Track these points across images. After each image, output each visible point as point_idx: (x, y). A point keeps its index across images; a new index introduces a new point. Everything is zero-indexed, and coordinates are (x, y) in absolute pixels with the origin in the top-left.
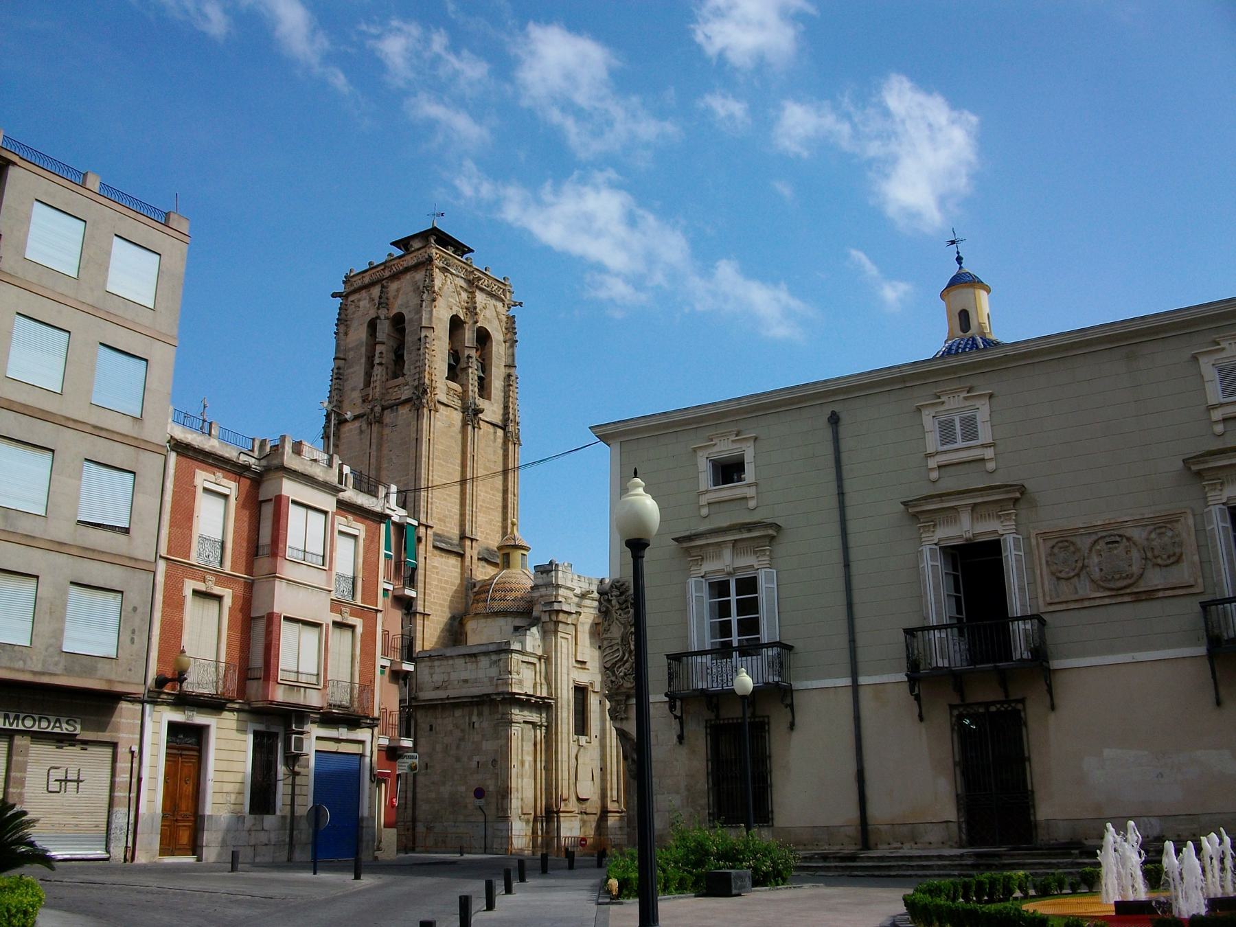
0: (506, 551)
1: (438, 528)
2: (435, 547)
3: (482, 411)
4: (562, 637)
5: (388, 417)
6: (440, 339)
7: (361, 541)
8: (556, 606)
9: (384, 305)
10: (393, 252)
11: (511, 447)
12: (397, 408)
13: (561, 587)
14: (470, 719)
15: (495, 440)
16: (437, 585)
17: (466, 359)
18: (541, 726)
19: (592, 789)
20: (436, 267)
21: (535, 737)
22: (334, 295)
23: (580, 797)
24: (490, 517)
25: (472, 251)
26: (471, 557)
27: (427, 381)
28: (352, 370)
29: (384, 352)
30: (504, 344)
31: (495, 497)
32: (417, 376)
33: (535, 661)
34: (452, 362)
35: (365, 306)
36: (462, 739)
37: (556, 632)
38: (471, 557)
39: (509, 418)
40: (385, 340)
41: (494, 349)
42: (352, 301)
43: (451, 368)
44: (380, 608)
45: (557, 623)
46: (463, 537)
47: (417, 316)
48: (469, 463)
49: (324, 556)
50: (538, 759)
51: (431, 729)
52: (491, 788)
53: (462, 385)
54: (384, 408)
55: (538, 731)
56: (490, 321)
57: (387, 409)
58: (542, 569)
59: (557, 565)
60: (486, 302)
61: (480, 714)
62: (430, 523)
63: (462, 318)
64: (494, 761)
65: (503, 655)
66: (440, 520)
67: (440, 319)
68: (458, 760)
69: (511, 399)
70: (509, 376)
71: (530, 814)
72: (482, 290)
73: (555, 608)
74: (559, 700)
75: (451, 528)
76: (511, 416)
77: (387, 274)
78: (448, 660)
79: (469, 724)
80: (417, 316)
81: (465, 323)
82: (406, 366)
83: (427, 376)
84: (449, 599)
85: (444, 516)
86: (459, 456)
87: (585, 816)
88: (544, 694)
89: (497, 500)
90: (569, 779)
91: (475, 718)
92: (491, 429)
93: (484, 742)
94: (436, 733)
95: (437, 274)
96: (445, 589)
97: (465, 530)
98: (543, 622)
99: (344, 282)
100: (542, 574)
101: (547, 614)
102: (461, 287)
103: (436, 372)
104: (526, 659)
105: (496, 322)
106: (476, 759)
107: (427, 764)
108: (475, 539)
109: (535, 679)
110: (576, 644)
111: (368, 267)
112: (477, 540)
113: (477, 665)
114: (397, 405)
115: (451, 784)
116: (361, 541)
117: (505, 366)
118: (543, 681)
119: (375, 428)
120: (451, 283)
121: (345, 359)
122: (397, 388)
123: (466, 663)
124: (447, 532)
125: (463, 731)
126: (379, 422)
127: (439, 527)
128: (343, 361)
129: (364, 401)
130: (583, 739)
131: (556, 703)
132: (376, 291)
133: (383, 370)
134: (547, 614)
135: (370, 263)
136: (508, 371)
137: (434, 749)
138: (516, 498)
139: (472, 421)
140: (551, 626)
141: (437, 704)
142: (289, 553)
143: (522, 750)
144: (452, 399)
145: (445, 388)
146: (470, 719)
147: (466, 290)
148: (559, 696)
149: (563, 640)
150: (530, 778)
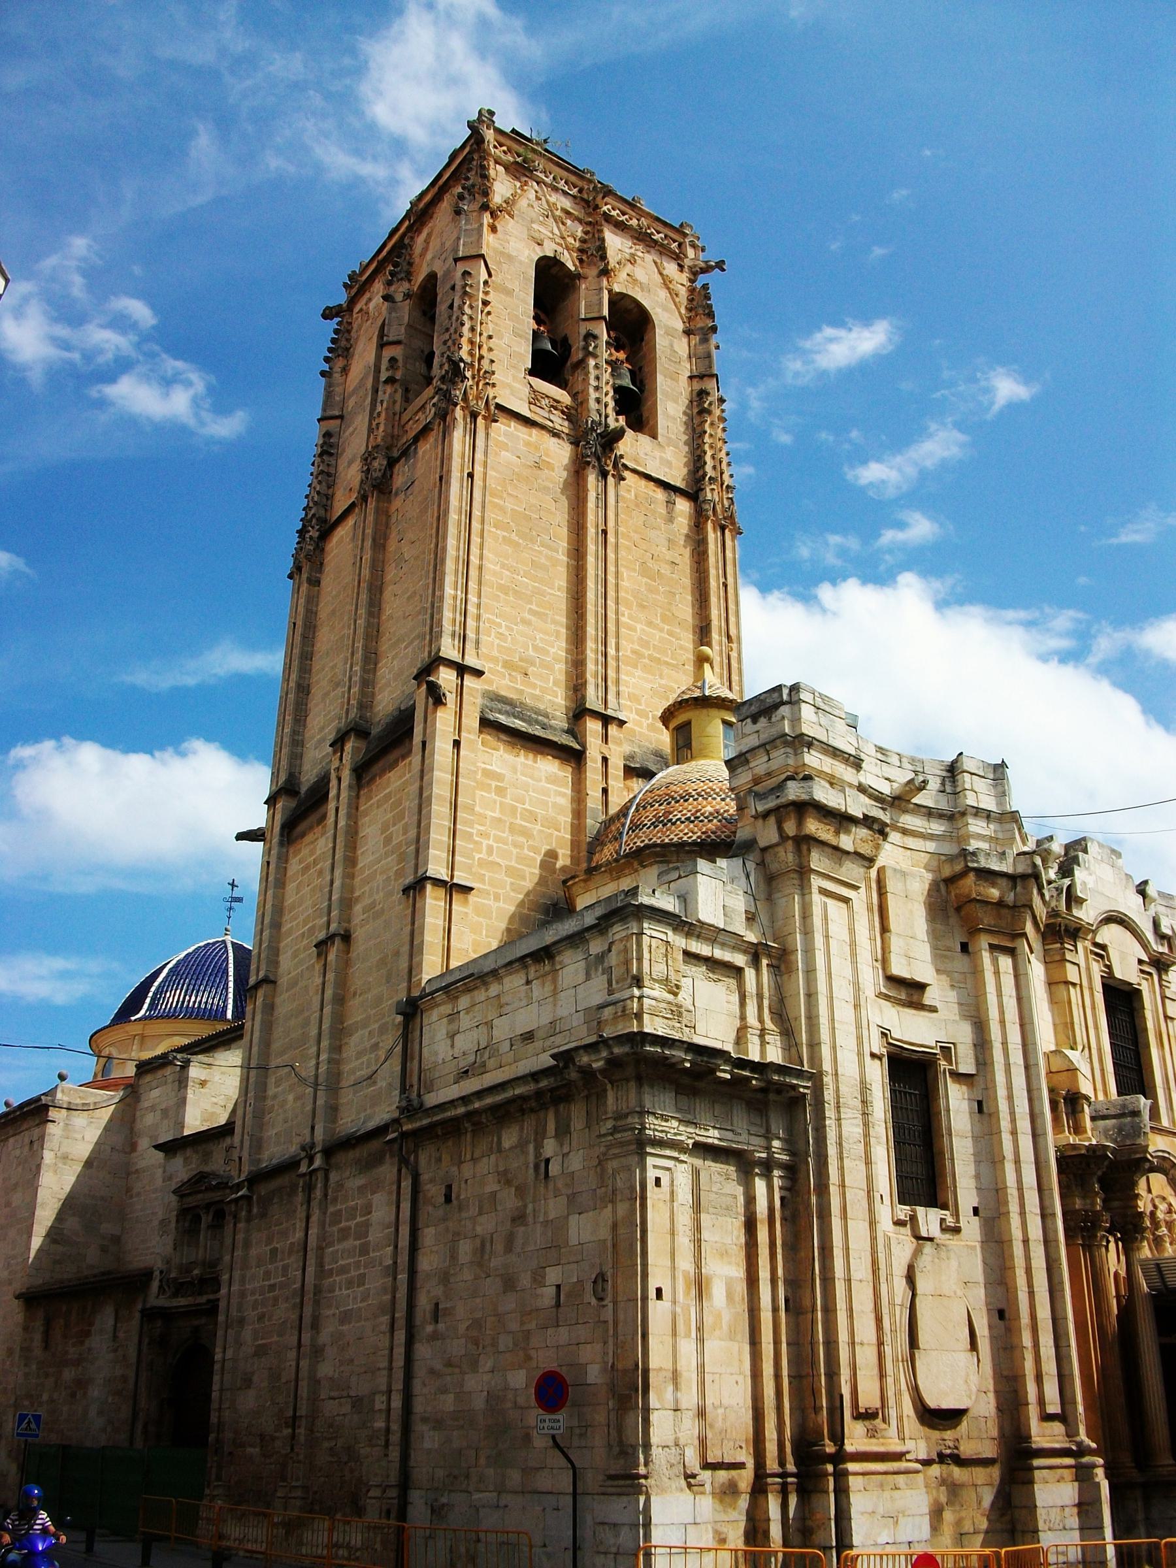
0: (681, 718)
1: (498, 681)
2: (486, 724)
4: (824, 892)
8: (794, 791)
9: (403, 275)
11: (712, 536)
12: (416, 449)
13: (810, 745)
14: (539, 1146)
15: (670, 519)
16: (500, 820)
17: (582, 343)
19: (974, 1379)
20: (496, 162)
21: (750, 1200)
22: (328, 314)
23: (932, 1403)
24: (663, 682)
26: (605, 760)
28: (351, 429)
29: (400, 358)
30: (685, 340)
31: (678, 639)
33: (739, 960)
36: (519, 1218)
37: (803, 872)
38: (605, 760)
39: (705, 474)
40: (402, 338)
42: (361, 310)
45: (804, 842)
46: (579, 713)
50: (764, 1274)
51: (448, 1199)
52: (594, 1374)
53: (574, 396)
55: (760, 1185)
58: (754, 709)
60: (632, 251)
61: (563, 1132)
62: (471, 661)
63: (573, 269)
64: (601, 1278)
65: (617, 928)
66: (508, 665)
68: (509, 1283)
69: (707, 439)
70: (702, 394)
71: (740, 1466)
72: (620, 227)
73: (792, 797)
74: (828, 1080)
75: (544, 690)
76: (710, 472)
78: (486, 984)
79: (536, 1167)
81: (579, 276)
84: (539, 859)
85: (521, 660)
87: (957, 1472)
88: (775, 1055)
89: (681, 647)
90: (880, 1343)
91: (550, 1147)
92: (660, 495)
93: (574, 1220)
94: (460, 1209)
95: (497, 173)
96: (526, 833)
97: (584, 697)
98: (764, 850)
99: (345, 285)
100: (755, 722)
101: (772, 820)
102: (567, 213)
104: (696, 947)
105: (663, 294)
106: (553, 1275)
107: (437, 1305)
108: (615, 718)
109: (743, 1018)
110: (885, 929)
112: (621, 723)
113: (554, 981)
115: (489, 1365)
117: (691, 378)
118: (769, 1024)
120: (538, 199)
121: (341, 417)
122: (420, 413)
123: (528, 982)
124: (534, 697)
125: (521, 1191)
127: (506, 682)
128: (338, 422)
130: (930, 1219)
131: (818, 1089)
133: (396, 391)
134: (772, 820)
136: (697, 386)
137: (454, 1256)
138: (734, 646)
139: (599, 459)
140: (787, 856)
141: (456, 1120)
143: (698, 1242)
144: (546, 415)
145: (527, 389)
146: (538, 1154)
147: (580, 221)
148: (827, 1066)
149: (830, 902)
150: (731, 1336)
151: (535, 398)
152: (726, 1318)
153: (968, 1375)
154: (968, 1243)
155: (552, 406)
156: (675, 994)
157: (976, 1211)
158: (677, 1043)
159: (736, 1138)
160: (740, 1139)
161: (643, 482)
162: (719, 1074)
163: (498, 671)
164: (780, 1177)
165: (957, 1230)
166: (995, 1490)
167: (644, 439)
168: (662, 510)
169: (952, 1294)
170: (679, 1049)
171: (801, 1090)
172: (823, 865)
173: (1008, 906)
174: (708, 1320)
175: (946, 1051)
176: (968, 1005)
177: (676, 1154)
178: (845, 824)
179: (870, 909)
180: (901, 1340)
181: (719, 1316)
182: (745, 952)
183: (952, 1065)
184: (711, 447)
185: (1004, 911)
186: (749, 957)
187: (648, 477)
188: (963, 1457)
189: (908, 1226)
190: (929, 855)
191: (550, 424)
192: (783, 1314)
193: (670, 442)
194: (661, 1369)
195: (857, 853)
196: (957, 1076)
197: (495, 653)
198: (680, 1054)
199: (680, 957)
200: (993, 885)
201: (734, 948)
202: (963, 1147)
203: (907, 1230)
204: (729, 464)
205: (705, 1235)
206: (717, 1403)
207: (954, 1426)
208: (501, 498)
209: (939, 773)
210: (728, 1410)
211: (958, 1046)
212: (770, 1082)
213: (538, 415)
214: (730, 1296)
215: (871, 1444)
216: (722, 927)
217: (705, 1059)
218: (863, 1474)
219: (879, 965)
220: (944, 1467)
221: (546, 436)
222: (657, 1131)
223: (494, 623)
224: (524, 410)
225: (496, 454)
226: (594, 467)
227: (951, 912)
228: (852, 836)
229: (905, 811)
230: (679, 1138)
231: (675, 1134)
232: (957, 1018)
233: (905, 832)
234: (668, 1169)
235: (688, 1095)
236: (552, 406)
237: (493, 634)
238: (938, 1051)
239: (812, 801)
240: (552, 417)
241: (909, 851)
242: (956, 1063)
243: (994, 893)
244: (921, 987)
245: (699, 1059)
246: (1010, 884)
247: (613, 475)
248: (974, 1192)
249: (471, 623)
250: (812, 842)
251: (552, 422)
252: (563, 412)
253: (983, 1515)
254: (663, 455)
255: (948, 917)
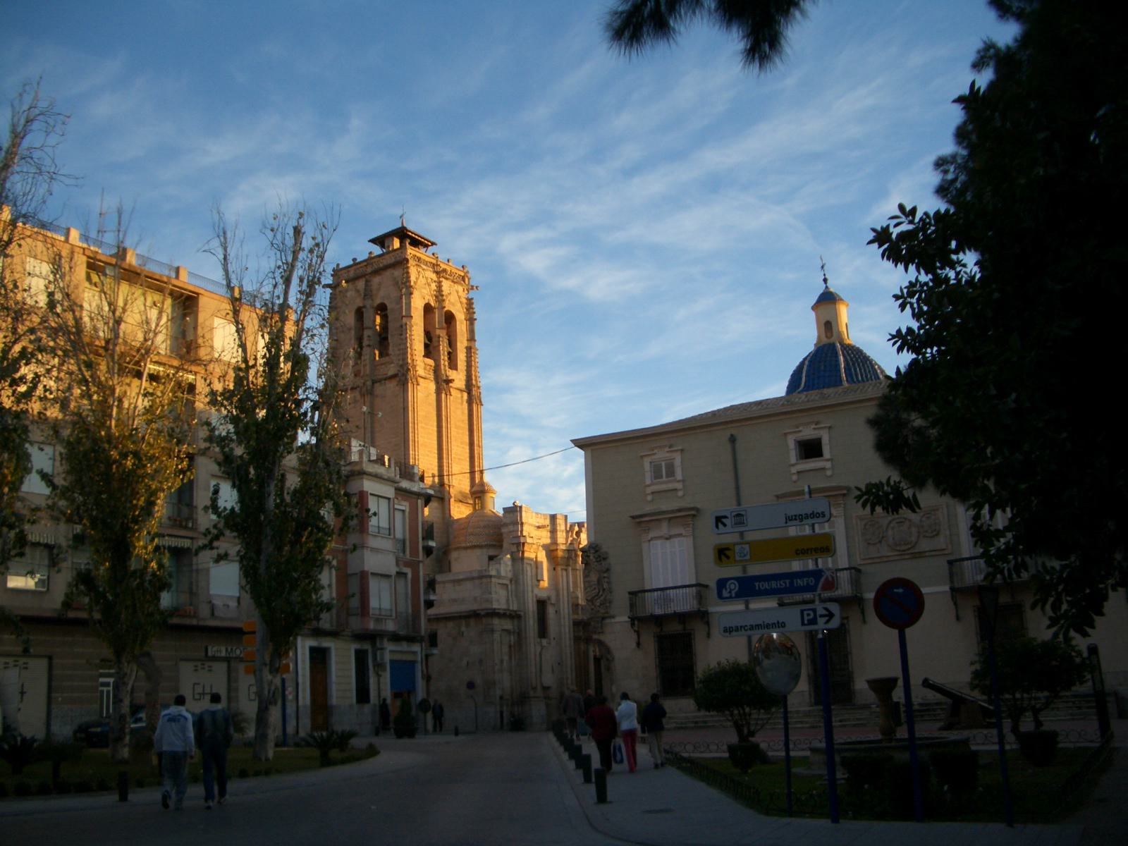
3: (452, 381)
5: (379, 389)
6: (417, 324)
7: (407, 514)
10: (373, 251)
18: (514, 632)
25: (435, 244)
27: (409, 361)
32: (401, 357)
34: (427, 342)
35: (354, 298)
41: (458, 327)
43: (426, 346)
44: (421, 559)
47: (398, 307)
48: (444, 424)
49: (389, 529)
53: (435, 360)
54: (374, 382)
56: (453, 305)
57: (376, 382)
59: (521, 507)
61: (468, 625)
64: (481, 661)
67: (416, 308)
76: (474, 382)
77: (369, 270)
80: (398, 307)
82: (391, 348)
83: (409, 356)
86: (435, 418)
91: (463, 629)
99: (332, 275)
101: (515, 546)
103: (416, 352)
104: (501, 581)
105: (459, 305)
111: (352, 263)
114: (385, 379)
116: (407, 514)
119: (368, 398)
126: (371, 394)
129: (356, 375)
130: (544, 642)
131: (525, 614)
132: (361, 284)
135: (354, 260)
142: (370, 529)
167: (455, 372)
175: (549, 598)
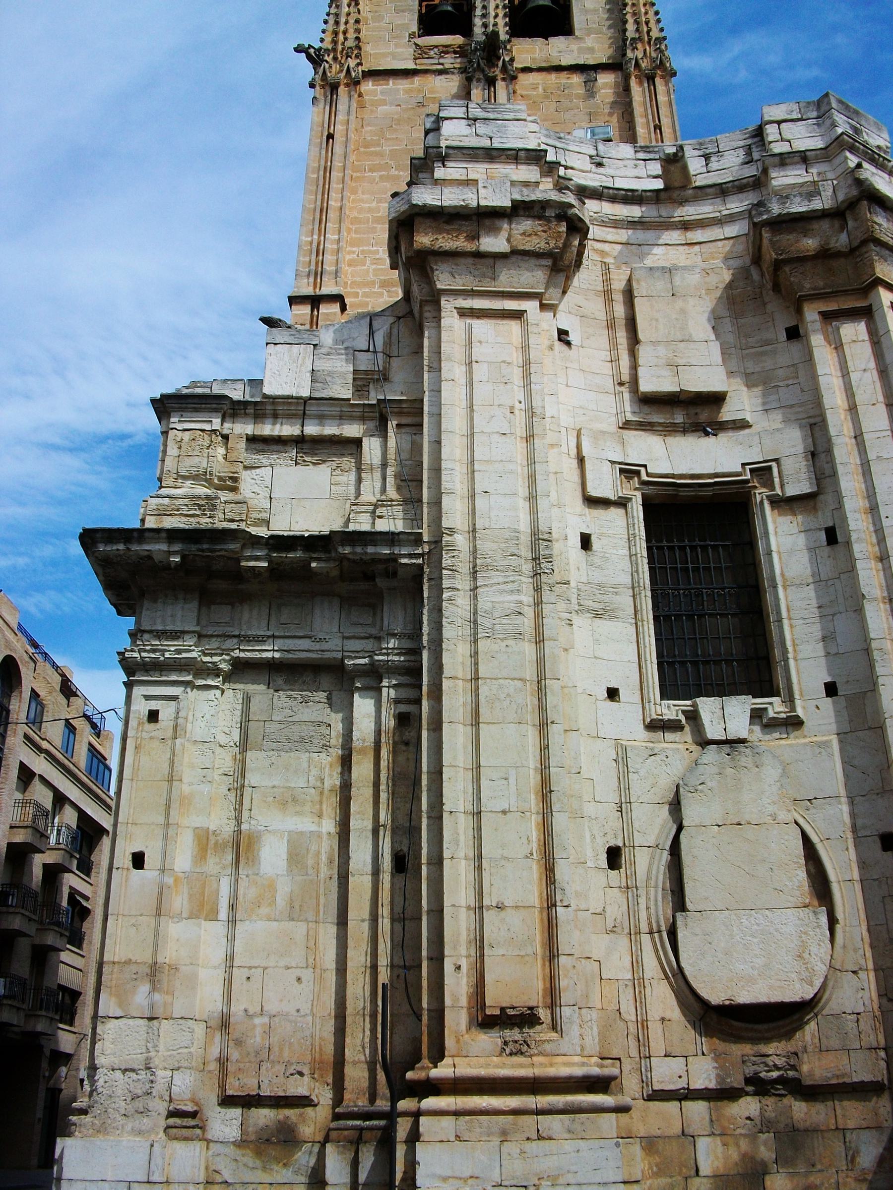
4: (463, 313)
23: (715, 995)
33: (352, 430)
71: (303, 1102)
87: (799, 1109)
92: (576, 79)
104: (267, 429)
144: (436, 61)
151: (421, 52)
152: (284, 889)
153: (804, 945)
154: (815, 739)
155: (442, 52)
156: (234, 489)
157: (831, 689)
158: (147, 534)
159: (317, 646)
160: (325, 646)
161: (553, 77)
162: (243, 564)
163: (375, 293)
164: (395, 686)
165: (794, 723)
166: (885, 1138)
168: (581, 91)
169: (769, 820)
170: (157, 541)
171: (404, 561)
172: (461, 282)
173: (838, 254)
174: (248, 893)
175: (762, 472)
176: (801, 405)
177: (189, 678)
178: (487, 222)
179: (611, 325)
180: (648, 899)
181: (271, 887)
182: (363, 419)
183: (773, 489)
184: (634, 14)
185: (835, 264)
186: (372, 424)
187: (558, 69)
188: (808, 1082)
189: (687, 729)
190: (731, 241)
191: (441, 67)
192: (386, 878)
193: (589, 32)
194: (129, 962)
195: (515, 252)
196: (783, 503)
197: (371, 277)
198: (159, 547)
199: (242, 445)
200: (806, 233)
201: (341, 418)
202: (802, 599)
203: (687, 735)
204: (658, 21)
205: (252, 778)
206: (254, 1009)
207: (788, 1035)
208: (378, 145)
209: (742, 143)
210: (276, 1019)
211: (783, 462)
212: (343, 558)
213: (424, 64)
214: (295, 858)
215: (504, 1066)
216: (306, 393)
217: (205, 546)
218: (457, 1113)
219: (625, 390)
220: (770, 1101)
221: (430, 78)
222: (145, 651)
223: (370, 252)
224: (411, 65)
225: (372, 111)
226: (479, 80)
227: (769, 295)
228: (504, 234)
229: (683, 202)
230: (184, 655)
231: (179, 652)
232: (780, 426)
233: (686, 226)
234: (174, 698)
235: (232, 605)
236: (442, 52)
237: (368, 262)
238: (749, 477)
239: (417, 210)
240: (441, 61)
241: (697, 248)
242: (782, 486)
243: (810, 244)
244: (716, 399)
245: (194, 547)
246: (837, 224)
247: (504, 79)
248: (823, 661)
249: (329, 258)
250: (431, 259)
251: (442, 64)
252: (455, 52)
253: (858, 1180)
254: (582, 45)
255: (765, 304)
